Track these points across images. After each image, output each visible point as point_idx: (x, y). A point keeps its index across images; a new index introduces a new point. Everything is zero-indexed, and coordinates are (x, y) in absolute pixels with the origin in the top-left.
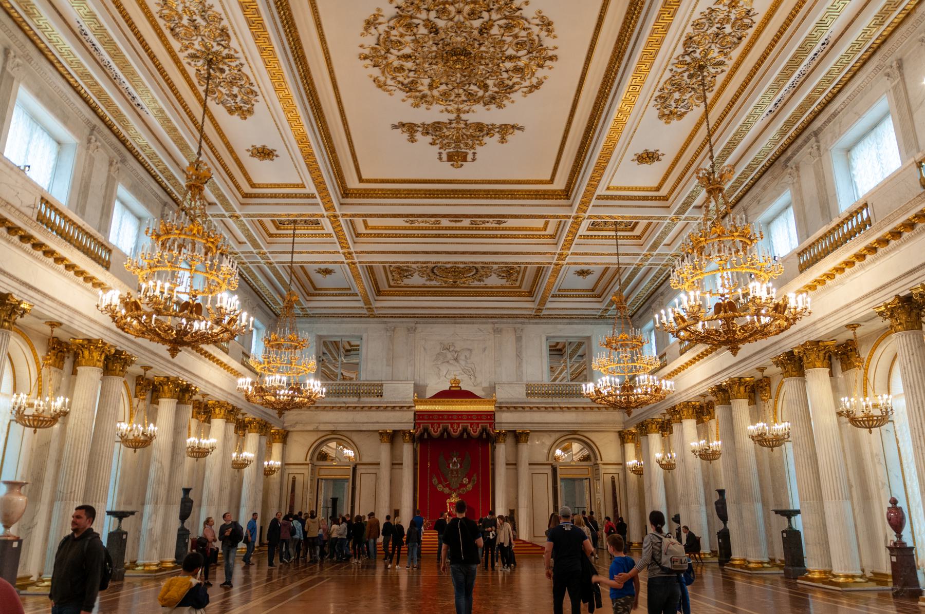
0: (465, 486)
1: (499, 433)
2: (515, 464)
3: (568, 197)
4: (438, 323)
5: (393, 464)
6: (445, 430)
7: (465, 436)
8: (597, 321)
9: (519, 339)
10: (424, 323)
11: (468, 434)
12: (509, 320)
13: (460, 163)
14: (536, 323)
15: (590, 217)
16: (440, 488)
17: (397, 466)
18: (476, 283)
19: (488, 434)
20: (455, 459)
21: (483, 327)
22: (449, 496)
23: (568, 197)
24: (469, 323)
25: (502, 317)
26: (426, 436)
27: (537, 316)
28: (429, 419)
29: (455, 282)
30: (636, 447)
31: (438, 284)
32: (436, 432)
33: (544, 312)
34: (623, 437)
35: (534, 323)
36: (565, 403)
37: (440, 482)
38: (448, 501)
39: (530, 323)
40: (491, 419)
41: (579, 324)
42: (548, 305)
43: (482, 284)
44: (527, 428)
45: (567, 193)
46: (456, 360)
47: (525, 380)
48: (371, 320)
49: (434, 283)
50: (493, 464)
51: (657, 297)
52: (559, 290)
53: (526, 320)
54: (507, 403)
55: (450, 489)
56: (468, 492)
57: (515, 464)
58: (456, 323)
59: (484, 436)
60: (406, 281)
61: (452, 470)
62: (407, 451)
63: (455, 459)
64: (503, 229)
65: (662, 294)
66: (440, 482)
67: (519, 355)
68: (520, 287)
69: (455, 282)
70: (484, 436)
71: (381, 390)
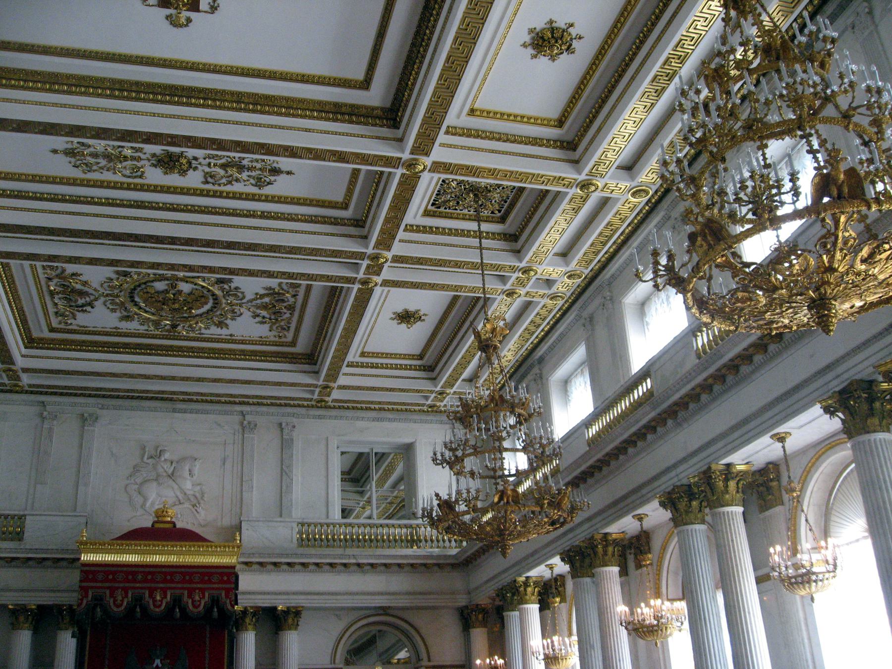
1: (245, 612)
3: (395, 125)
4: (143, 409)
6: (138, 600)
8: (424, 417)
9: (286, 444)
10: (115, 408)
12: (273, 409)
13: (185, 14)
14: (320, 417)
15: (437, 167)
18: (214, 331)
19: (222, 611)
21: (221, 419)
23: (395, 125)
24: (197, 412)
25: (259, 401)
27: (321, 404)
29: (174, 326)
30: (490, 634)
31: (142, 329)
32: (119, 603)
33: (336, 395)
34: (468, 617)
35: (315, 417)
36: (367, 557)
39: (308, 417)
41: (394, 420)
42: (342, 380)
43: (224, 332)
45: (391, 116)
46: (171, 476)
47: (298, 513)
48: (15, 397)
49: (133, 326)
51: (531, 367)
52: (363, 354)
53: (302, 411)
54: (260, 555)
58: (174, 411)
60: (82, 319)
62: (67, 646)
64: (268, 199)
65: (541, 360)
67: (284, 472)
68: (293, 344)
69: (174, 326)
71: (22, 527)
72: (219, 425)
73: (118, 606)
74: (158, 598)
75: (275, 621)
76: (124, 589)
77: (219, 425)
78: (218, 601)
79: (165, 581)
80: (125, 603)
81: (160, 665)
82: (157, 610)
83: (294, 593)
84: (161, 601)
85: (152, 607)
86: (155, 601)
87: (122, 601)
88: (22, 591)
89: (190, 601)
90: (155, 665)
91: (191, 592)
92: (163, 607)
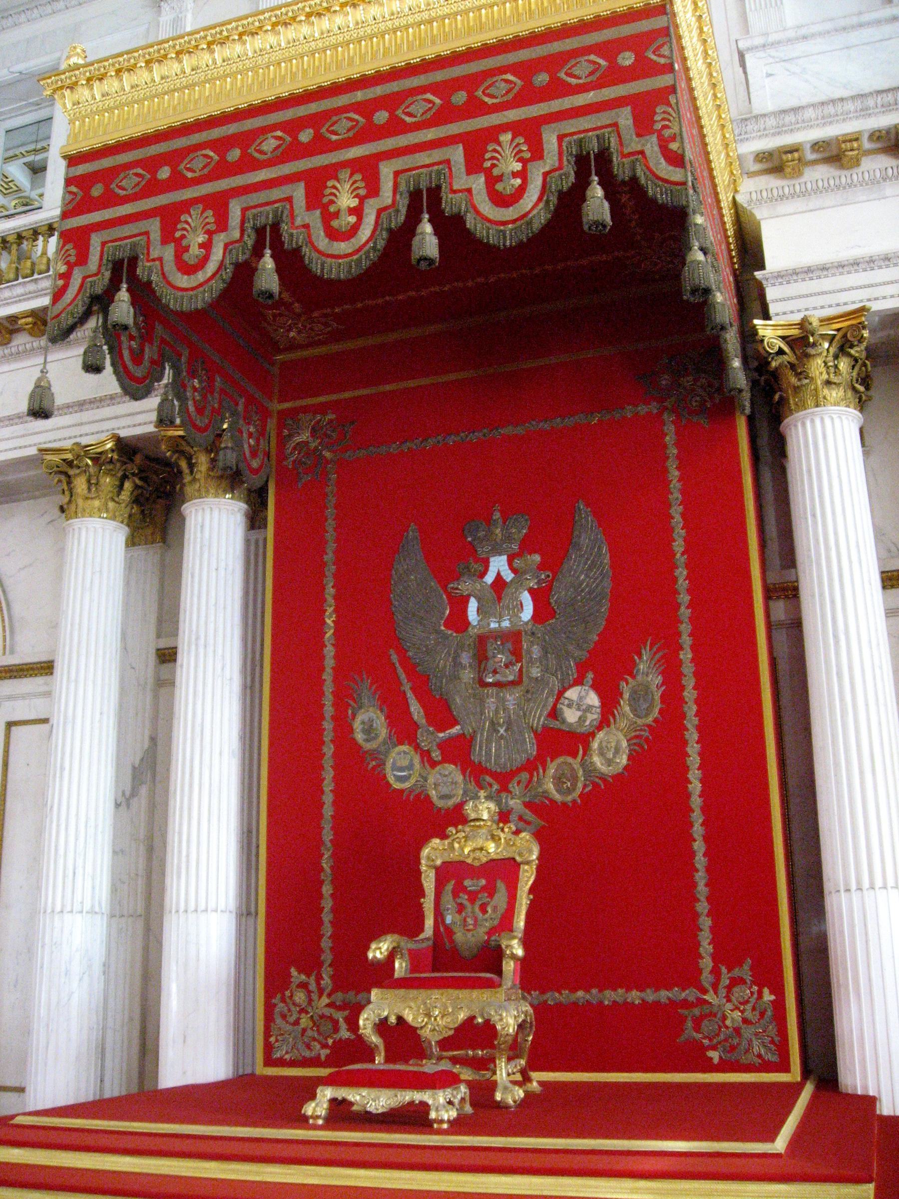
1: (801, 341)
11: (451, 228)
16: (401, 768)
20: (499, 565)
28: (152, 188)
40: (644, 69)
50: (787, 591)
55: (476, 773)
56: (605, 793)
61: (482, 640)
63: (499, 565)
66: (404, 730)
73: (188, 269)
74: (346, 200)
76: (207, 201)
78: (603, 158)
80: (217, 254)
81: (508, 576)
84: (357, 211)
85: (322, 242)
86: (328, 217)
87: (207, 246)
89: (478, 183)
90: (489, 578)
91: (476, 148)
92: (365, 232)
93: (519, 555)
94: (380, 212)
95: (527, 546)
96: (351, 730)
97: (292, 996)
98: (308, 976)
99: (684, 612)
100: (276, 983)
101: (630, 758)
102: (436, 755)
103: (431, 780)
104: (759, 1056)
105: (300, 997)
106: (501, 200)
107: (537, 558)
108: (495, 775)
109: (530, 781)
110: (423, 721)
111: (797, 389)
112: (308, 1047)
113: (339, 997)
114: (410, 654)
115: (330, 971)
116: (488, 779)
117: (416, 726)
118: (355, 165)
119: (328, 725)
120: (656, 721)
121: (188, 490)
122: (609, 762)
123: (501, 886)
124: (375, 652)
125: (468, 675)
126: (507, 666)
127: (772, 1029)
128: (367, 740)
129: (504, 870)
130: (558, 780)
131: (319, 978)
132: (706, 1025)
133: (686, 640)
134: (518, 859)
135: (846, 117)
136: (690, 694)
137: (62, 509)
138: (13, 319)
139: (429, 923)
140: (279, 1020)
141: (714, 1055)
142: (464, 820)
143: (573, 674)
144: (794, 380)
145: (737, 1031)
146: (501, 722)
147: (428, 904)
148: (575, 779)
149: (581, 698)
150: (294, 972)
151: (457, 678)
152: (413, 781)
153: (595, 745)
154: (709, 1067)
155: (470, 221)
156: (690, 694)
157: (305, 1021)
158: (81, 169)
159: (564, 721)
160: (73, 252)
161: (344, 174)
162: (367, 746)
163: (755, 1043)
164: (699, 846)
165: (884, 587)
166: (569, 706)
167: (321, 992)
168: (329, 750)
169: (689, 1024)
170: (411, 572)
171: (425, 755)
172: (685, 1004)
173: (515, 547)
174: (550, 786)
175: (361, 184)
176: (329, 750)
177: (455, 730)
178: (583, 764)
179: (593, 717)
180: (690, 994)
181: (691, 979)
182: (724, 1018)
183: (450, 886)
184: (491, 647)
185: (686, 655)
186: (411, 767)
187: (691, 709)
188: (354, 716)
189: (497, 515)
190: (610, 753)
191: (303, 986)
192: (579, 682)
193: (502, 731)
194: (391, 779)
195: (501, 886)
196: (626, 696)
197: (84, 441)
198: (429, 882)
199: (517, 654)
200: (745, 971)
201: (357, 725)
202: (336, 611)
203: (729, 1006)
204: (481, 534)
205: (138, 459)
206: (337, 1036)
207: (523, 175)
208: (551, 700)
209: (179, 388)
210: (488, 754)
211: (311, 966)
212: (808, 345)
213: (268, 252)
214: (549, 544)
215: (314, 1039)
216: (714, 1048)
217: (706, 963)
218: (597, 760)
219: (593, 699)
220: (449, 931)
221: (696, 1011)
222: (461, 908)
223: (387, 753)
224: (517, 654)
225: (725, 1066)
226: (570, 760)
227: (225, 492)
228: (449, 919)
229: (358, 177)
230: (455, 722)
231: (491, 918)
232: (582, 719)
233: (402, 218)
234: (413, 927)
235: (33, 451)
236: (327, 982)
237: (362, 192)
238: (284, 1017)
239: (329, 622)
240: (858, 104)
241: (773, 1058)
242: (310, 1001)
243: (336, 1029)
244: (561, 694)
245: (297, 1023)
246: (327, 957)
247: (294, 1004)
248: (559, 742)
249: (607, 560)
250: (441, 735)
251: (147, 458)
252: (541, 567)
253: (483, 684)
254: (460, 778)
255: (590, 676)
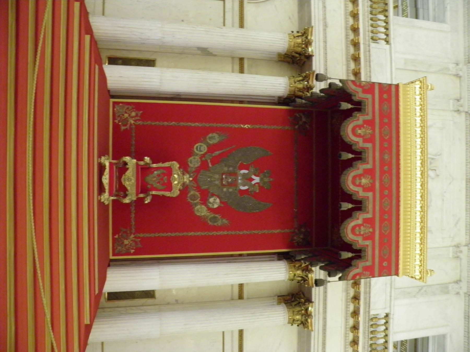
0: (204, 201)
2: (241, 297)
5: (241, 60)
7: (346, 206)
16: (200, 148)
17: (237, 67)
20: (257, 180)
22: (184, 167)
26: (345, 106)
37: (211, 149)
38: (175, 165)
44: (316, 322)
55: (198, 170)
56: (190, 207)
57: (241, 297)
59: (346, 255)
63: (257, 180)
66: (211, 149)
70: (346, 255)
72: (457, 223)
75: (296, 299)
77: (457, 223)
79: (382, 188)
81: (253, 182)
82: (350, 179)
83: (325, 319)
86: (360, 176)
87: (359, 136)
88: (325, 42)
89: (360, 222)
90: (253, 177)
93: (259, 186)
94: (358, 192)
95: (261, 188)
96: (213, 132)
97: (133, 111)
98: (140, 117)
99: (238, 232)
100: (138, 107)
101: (199, 216)
102: (203, 159)
103: (197, 157)
104: (117, 248)
105: (133, 114)
106: (353, 229)
107: (257, 191)
108: (196, 177)
109: (194, 187)
110: (214, 155)
111: (295, 266)
112: (119, 116)
113: (134, 127)
114: (234, 152)
115: (141, 124)
116: (196, 174)
117: (212, 153)
118: (373, 185)
119: (215, 125)
120: (208, 224)
121: (292, 80)
122: (198, 210)
123: (165, 187)
124: (235, 141)
125: (226, 169)
126: (228, 182)
127: (124, 252)
128: (210, 138)
129: (169, 187)
130: (194, 195)
131: (139, 120)
132: (125, 235)
133: (230, 233)
134: (172, 191)
135: (365, 288)
136: (215, 233)
137: (293, 32)
138: (358, 20)
139: (154, 165)
140: (127, 107)
141: (116, 237)
142: (183, 174)
143: (224, 200)
144: (297, 266)
145: (123, 243)
146: (212, 178)
147: (161, 165)
148: (194, 200)
149: (216, 203)
150: (141, 112)
151: (226, 166)
152: (196, 152)
153: (203, 206)
154: (114, 234)
155: (349, 220)
156: (215, 233)
157: (126, 115)
158: (393, 89)
159: (210, 198)
160: (367, 88)
161: (371, 181)
162: (208, 137)
163: (120, 248)
164: (173, 235)
165: (239, 284)
166: (215, 200)
167: (135, 121)
168: (207, 125)
169: (125, 230)
170: (257, 152)
171: (203, 156)
172: (131, 229)
173: (261, 185)
174: (192, 193)
175: (367, 186)
176: (207, 125)
177: (210, 165)
178: (197, 203)
179: (210, 205)
180: (133, 231)
181: (137, 231)
182: (127, 239)
183: (165, 172)
184: (233, 177)
185: (225, 233)
186: (201, 151)
187: (211, 234)
188: (217, 133)
189: (271, 179)
190: (201, 211)
191: (137, 115)
192: (221, 202)
193: (209, 179)
194: (197, 145)
195: (165, 187)
196: (217, 216)
197: (313, 44)
198: (167, 164)
199: (230, 185)
200: (139, 246)
201: (215, 135)
202: (249, 128)
203: (130, 240)
204: (267, 175)
205: (306, 60)
206: (121, 126)
207: (360, 235)
208: (216, 194)
209: (322, 97)
210: (202, 175)
211: (143, 117)
212: (306, 271)
213: (353, 156)
214: (261, 194)
215: (121, 118)
216: (119, 236)
217: (142, 235)
218: (199, 207)
219: (216, 206)
220: (152, 173)
221: (128, 232)
222: (159, 175)
223: (204, 144)
224: (230, 185)
225: (114, 240)
226: (199, 199)
227: (290, 92)
228: (156, 172)
229: (370, 185)
230: (213, 164)
231: (156, 185)
232: (210, 203)
233: (354, 199)
234: (153, 163)
235: (313, 24)
236: (139, 123)
237: (365, 186)
238: (128, 108)
239: (246, 126)
240: (368, 292)
241: (116, 252)
242: (132, 117)
243: (125, 125)
244: (218, 197)
245: (126, 113)
246: (146, 123)
247: (131, 112)
248: (205, 196)
249: (254, 211)
250: (209, 161)
251: (304, 62)
252: (255, 192)
253: (223, 174)
254: (196, 166)
255: (222, 205)
